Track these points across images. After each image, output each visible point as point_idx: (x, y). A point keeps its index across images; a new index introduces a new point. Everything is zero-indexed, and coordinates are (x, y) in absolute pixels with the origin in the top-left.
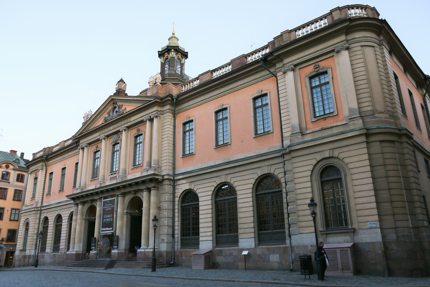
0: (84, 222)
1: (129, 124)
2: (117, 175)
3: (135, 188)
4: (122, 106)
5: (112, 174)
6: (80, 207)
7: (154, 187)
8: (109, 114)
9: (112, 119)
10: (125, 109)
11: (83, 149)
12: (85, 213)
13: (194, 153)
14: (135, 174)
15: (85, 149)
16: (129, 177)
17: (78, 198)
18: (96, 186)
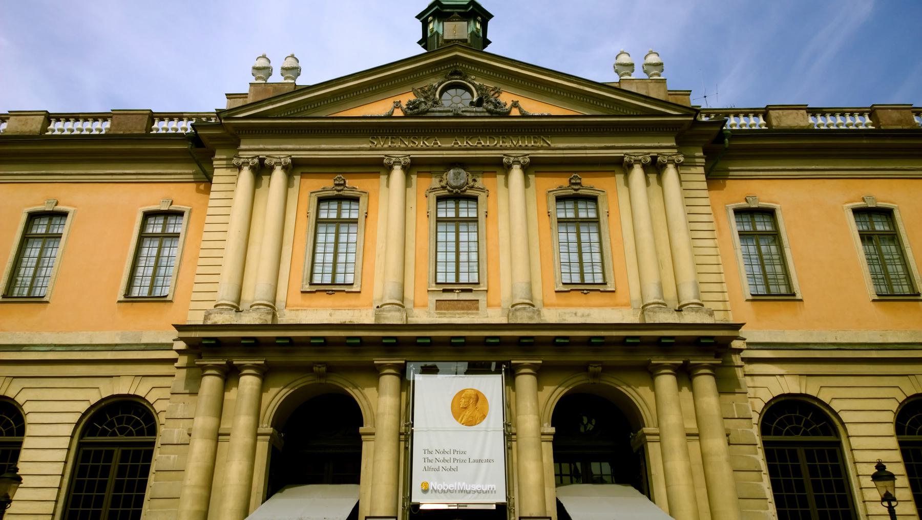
0: (263, 447)
1: (541, 153)
2: (482, 298)
3: (616, 357)
4: (499, 92)
5: (444, 291)
6: (249, 383)
7: (712, 367)
8: (427, 94)
9: (457, 116)
10: (515, 105)
11: (261, 170)
12: (268, 413)
13: (799, 296)
14: (580, 311)
15: (278, 175)
16: (551, 316)
17: (254, 346)
18: (377, 316)
